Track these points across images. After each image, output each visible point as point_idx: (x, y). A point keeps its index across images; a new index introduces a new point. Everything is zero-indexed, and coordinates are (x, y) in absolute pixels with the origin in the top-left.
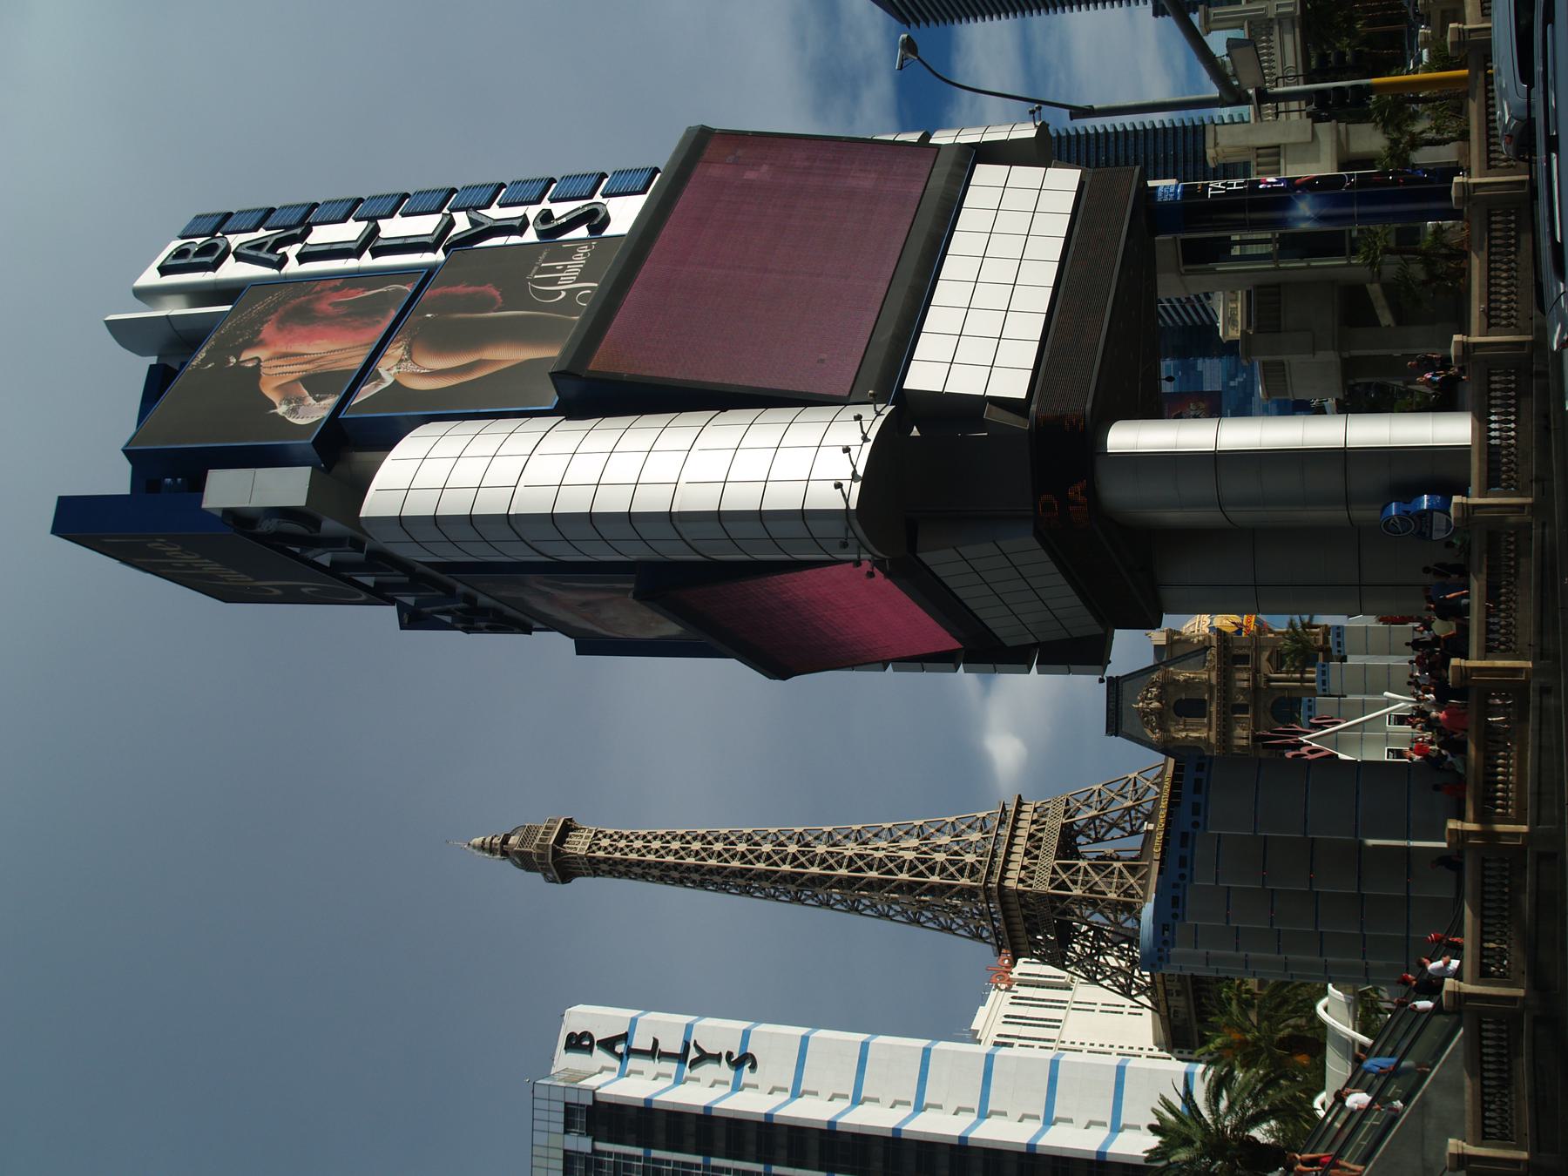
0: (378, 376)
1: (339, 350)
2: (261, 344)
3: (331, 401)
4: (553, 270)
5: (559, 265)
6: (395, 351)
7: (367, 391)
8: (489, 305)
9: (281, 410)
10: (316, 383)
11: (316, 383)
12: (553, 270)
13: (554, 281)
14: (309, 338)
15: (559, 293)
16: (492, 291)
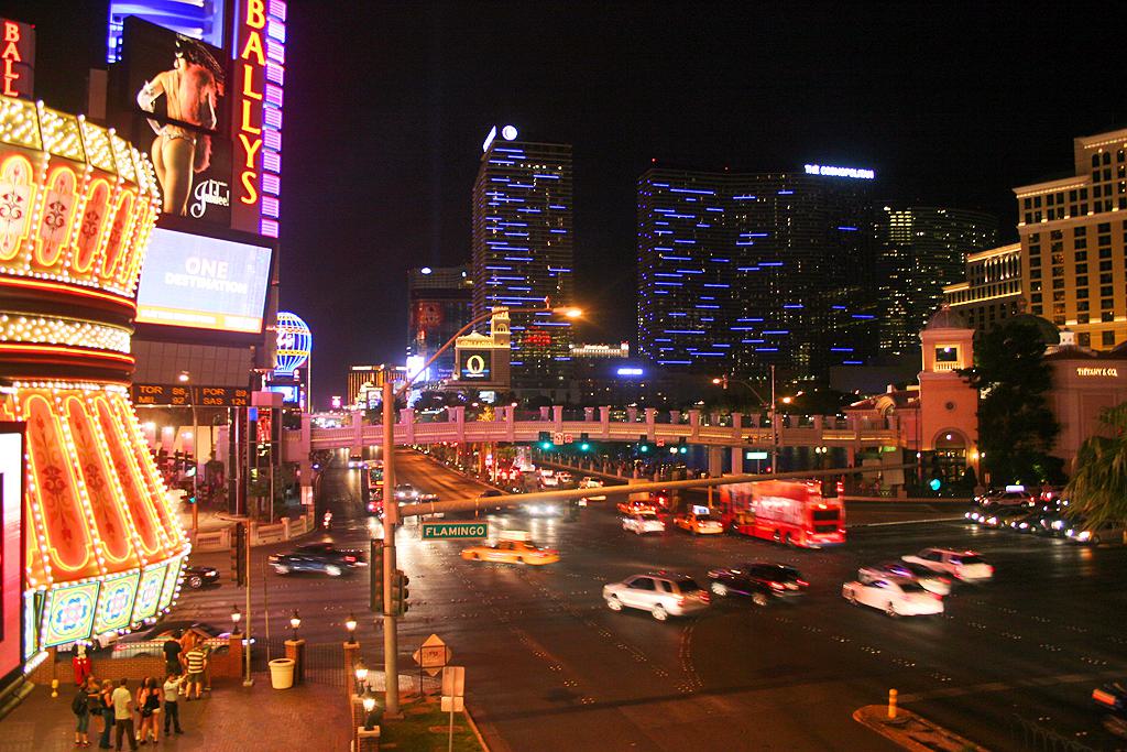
0: (162, 126)
1: (179, 106)
2: (188, 66)
3: (151, 109)
4: (214, 189)
5: (217, 192)
6: (175, 132)
7: (154, 124)
8: (197, 164)
9: (148, 87)
10: (162, 101)
11: (162, 101)
12: (214, 189)
13: (207, 192)
14: (189, 88)
15: (199, 194)
16: (206, 164)
